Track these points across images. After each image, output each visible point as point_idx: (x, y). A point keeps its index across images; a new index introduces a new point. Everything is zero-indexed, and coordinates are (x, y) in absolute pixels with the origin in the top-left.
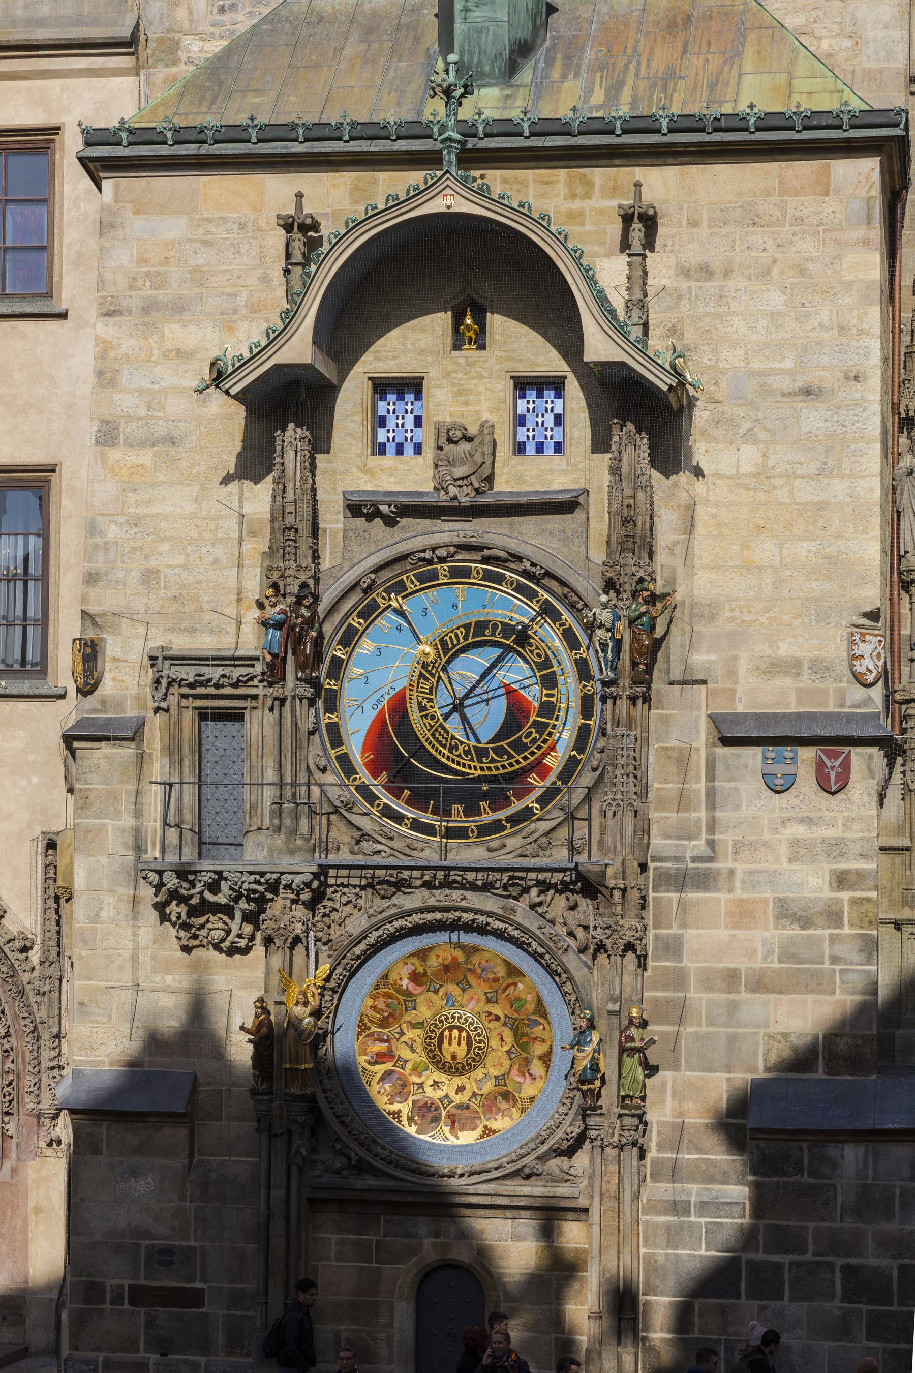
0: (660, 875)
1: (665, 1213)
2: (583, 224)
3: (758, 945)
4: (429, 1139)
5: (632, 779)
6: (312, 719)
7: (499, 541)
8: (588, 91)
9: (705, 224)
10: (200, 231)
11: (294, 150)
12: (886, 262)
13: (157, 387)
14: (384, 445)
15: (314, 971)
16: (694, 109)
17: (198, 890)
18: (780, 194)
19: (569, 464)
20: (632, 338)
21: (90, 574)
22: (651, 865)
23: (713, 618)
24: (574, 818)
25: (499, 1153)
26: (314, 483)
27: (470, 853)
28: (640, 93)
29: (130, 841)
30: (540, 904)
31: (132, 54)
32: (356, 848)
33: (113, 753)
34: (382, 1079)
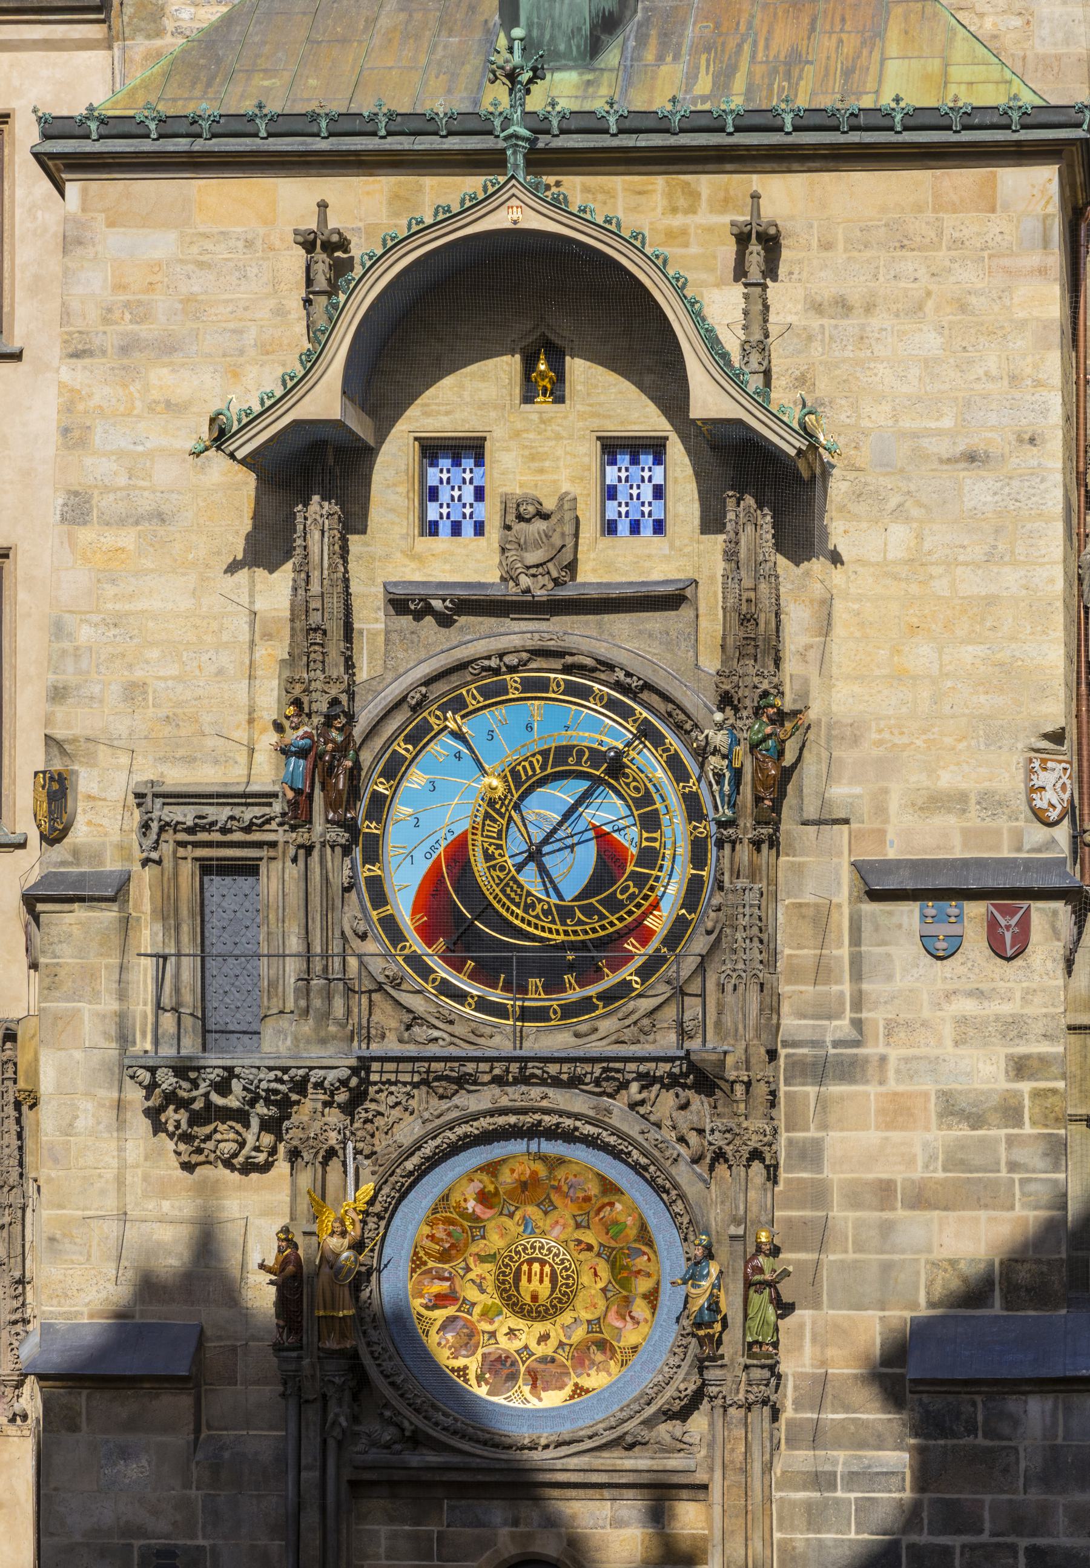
0: (794, 1064)
1: (805, 1488)
3: (918, 1150)
4: (505, 1402)
5: (756, 943)
6: (347, 872)
7: (585, 645)
8: (692, 77)
9: (841, 246)
10: (195, 249)
11: (314, 147)
12: (1067, 296)
13: (140, 448)
14: (436, 523)
15: (355, 1193)
16: (825, 101)
17: (202, 1090)
18: (935, 211)
19: (672, 547)
20: (751, 389)
21: (56, 688)
22: (783, 1052)
23: (856, 741)
24: (684, 994)
25: (594, 1418)
26: (346, 571)
27: (553, 1040)
28: (758, 80)
29: (113, 1030)
30: (642, 1102)
31: (103, 21)
32: (406, 1034)
33: (90, 918)
34: (443, 1328)
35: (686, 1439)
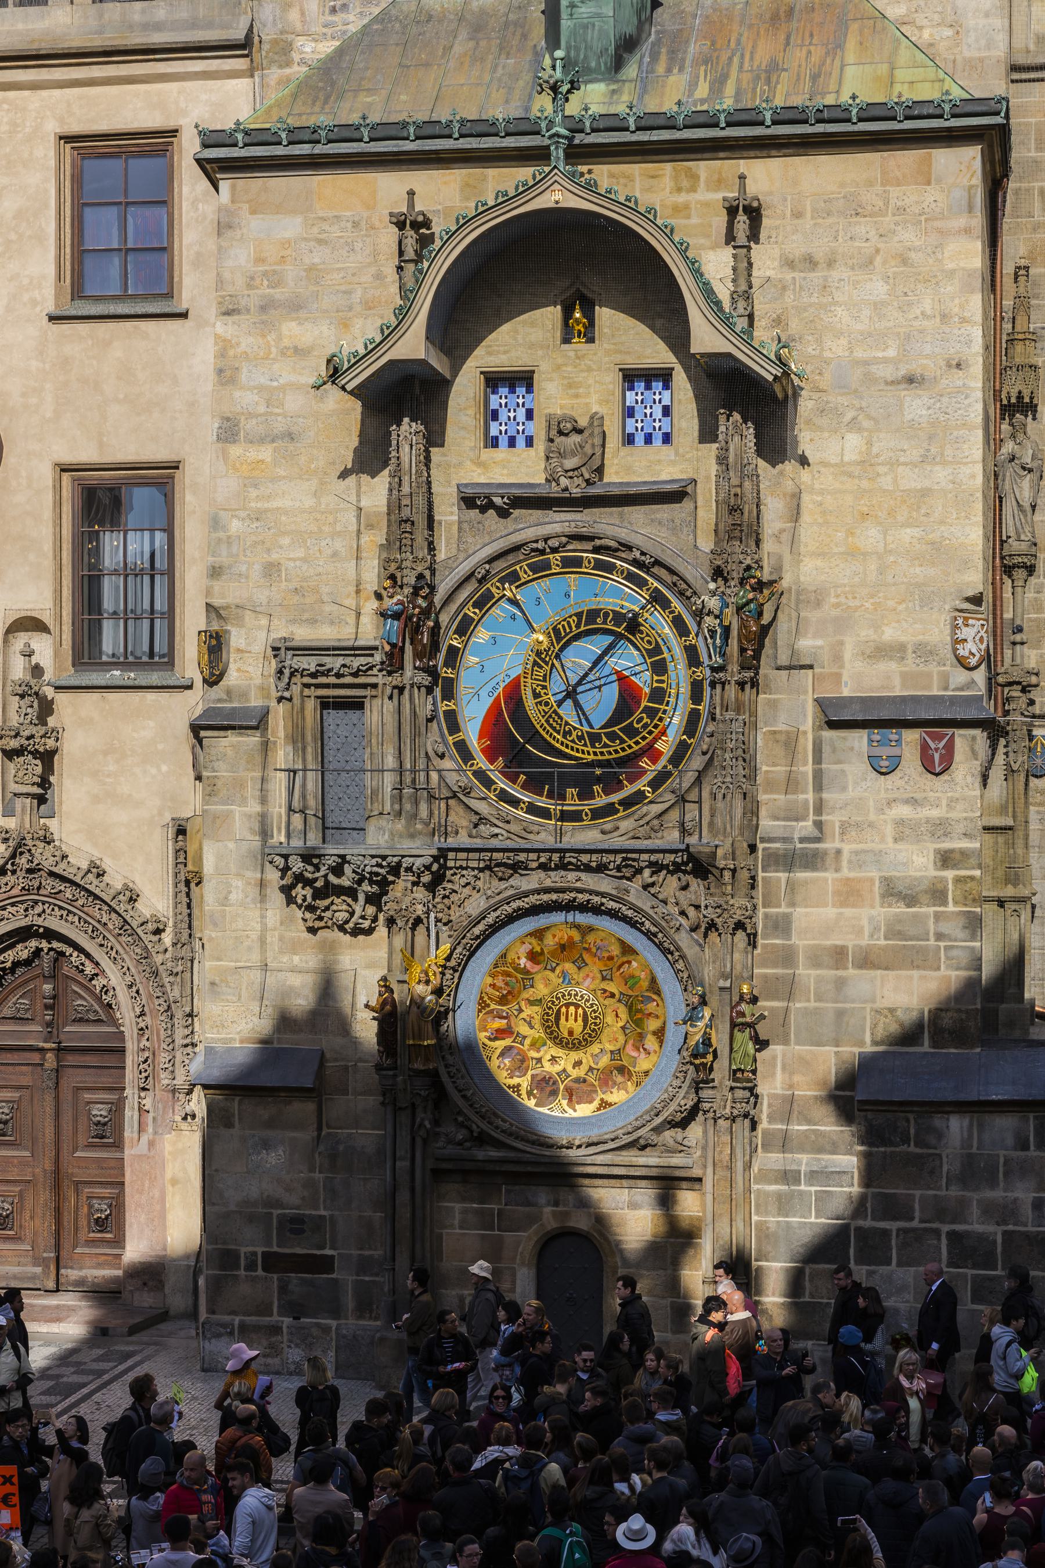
1: (776, 1182)
2: (688, 217)
3: (865, 922)
5: (740, 762)
6: (430, 707)
7: (610, 531)
8: (693, 85)
9: (809, 215)
10: (315, 230)
11: (404, 149)
12: (987, 250)
13: (275, 384)
14: (497, 438)
15: (436, 952)
16: (797, 101)
17: (322, 873)
18: (883, 185)
19: (677, 454)
20: (738, 329)
21: (214, 568)
22: (760, 846)
23: (818, 604)
24: (685, 801)
25: (615, 1125)
26: (429, 476)
27: (584, 836)
28: (744, 85)
29: (257, 826)
30: (653, 884)
31: (246, 56)
32: (474, 831)
34: (502, 1055)
35: (685, 1142)
